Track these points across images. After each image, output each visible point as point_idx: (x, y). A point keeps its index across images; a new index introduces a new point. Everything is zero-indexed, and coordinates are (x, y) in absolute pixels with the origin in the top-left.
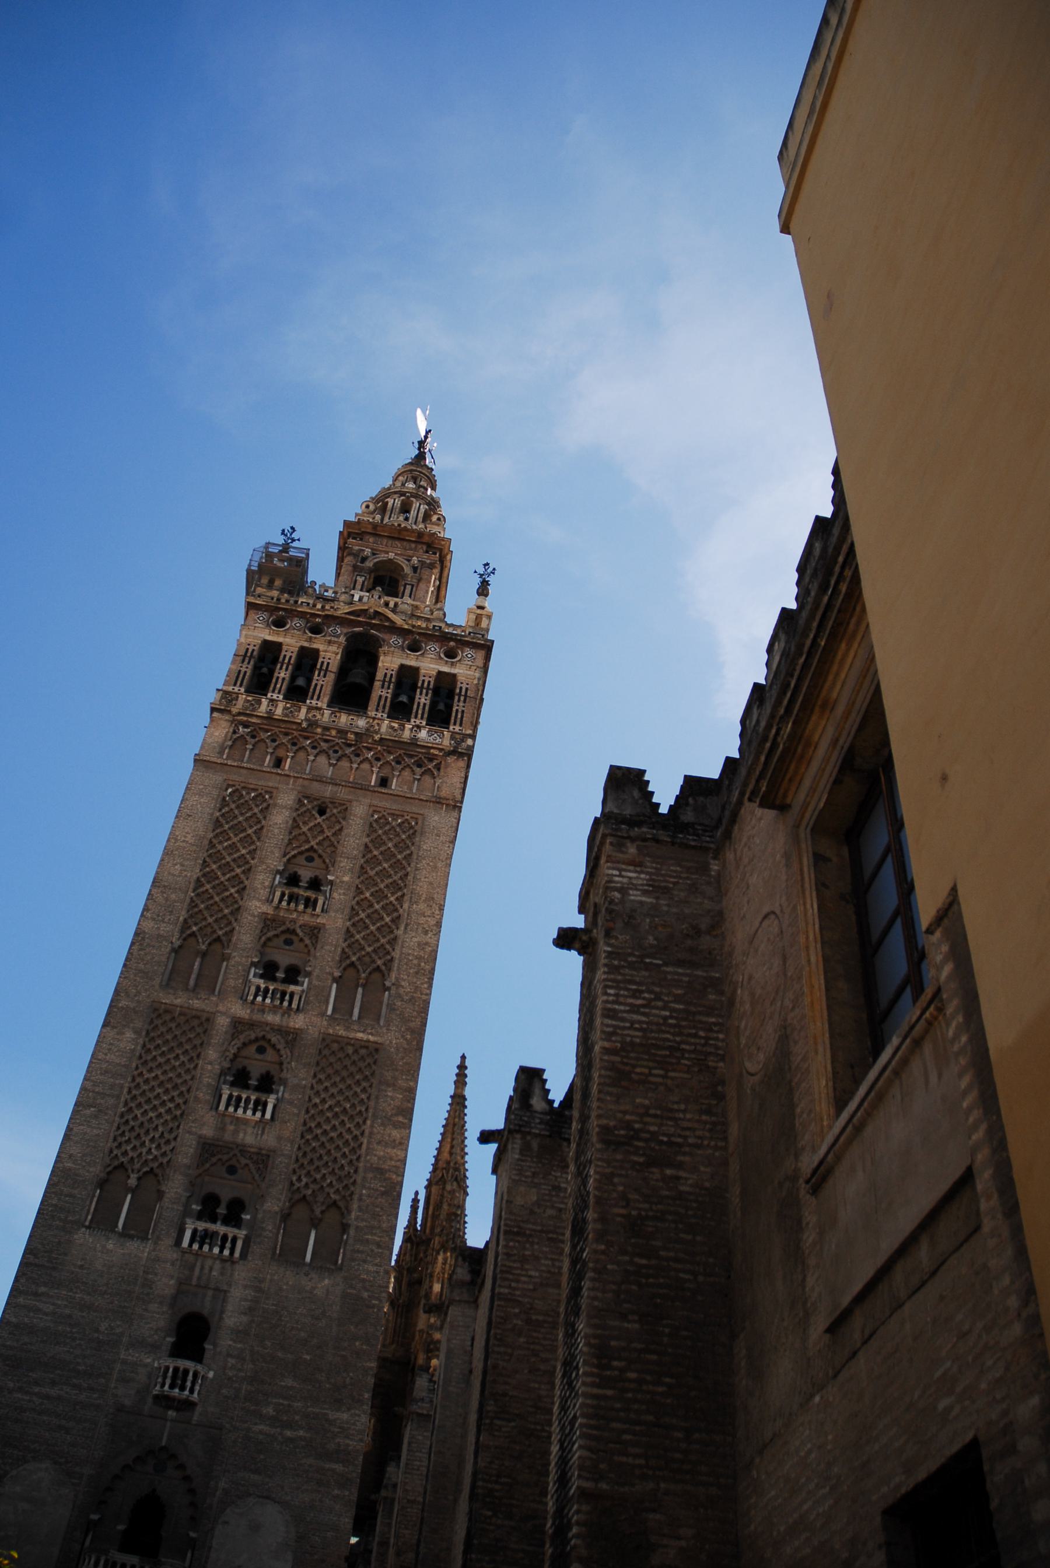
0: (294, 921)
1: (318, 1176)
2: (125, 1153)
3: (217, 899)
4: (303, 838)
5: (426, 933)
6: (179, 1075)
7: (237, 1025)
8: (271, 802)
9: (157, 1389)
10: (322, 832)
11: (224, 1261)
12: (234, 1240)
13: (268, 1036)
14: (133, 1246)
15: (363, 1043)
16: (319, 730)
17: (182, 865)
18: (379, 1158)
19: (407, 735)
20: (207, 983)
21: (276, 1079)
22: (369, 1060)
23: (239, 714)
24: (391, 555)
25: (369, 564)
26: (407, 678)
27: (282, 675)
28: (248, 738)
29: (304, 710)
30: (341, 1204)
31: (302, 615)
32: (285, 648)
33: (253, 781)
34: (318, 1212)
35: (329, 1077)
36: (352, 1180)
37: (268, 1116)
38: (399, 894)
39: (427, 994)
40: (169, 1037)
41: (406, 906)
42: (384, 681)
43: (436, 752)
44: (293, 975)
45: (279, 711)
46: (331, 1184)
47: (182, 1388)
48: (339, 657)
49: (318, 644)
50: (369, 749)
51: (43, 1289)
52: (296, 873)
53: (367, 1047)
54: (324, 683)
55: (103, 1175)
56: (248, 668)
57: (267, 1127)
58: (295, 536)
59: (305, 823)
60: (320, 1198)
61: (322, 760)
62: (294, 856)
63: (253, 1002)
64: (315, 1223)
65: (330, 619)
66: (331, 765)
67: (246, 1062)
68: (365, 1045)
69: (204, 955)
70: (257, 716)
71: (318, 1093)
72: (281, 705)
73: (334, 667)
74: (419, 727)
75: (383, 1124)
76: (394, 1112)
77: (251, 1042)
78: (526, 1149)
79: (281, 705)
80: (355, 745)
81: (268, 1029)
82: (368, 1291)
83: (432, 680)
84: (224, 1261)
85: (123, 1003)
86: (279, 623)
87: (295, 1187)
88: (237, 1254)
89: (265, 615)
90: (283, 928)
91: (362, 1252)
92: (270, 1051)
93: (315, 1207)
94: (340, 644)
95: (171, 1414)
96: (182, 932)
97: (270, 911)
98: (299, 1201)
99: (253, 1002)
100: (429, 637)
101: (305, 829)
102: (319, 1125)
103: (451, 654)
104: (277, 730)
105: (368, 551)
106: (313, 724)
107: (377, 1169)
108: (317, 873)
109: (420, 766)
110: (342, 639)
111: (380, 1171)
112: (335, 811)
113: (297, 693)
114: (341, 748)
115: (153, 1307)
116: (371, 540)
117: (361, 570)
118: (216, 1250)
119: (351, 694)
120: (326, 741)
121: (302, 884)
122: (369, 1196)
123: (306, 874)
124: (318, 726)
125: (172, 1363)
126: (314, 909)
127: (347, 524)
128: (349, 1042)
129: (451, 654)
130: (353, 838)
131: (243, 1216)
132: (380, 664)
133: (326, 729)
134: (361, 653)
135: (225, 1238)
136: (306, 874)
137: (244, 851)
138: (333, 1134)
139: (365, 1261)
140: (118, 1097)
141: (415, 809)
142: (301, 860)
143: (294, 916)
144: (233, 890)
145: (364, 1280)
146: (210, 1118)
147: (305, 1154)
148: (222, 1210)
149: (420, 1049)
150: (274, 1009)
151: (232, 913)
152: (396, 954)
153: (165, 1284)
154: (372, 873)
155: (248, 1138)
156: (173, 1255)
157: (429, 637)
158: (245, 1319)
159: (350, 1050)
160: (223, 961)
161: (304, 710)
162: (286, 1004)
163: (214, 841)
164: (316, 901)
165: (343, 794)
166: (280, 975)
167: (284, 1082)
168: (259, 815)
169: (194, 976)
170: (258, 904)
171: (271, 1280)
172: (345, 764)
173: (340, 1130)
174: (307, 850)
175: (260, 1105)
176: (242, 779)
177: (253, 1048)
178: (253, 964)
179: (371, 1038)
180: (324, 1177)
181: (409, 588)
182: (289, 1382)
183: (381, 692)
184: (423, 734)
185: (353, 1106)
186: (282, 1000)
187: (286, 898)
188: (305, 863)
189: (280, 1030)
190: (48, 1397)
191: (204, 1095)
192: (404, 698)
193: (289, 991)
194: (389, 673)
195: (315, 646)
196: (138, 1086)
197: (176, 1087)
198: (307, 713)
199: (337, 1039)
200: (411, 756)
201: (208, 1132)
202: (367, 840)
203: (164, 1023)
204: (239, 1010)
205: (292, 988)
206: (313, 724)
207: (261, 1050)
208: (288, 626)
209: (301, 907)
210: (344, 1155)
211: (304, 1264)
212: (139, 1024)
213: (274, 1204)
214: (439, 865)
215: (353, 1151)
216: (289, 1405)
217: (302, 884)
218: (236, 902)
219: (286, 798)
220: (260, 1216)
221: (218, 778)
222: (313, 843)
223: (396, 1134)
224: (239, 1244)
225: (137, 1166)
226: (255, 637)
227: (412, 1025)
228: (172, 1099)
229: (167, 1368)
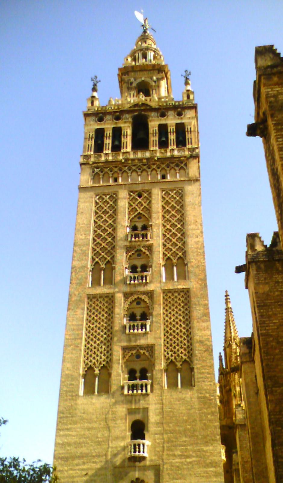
0: (139, 246)
1: (176, 350)
4: (134, 210)
8: (116, 198)
10: (142, 205)
12: (146, 385)
13: (140, 297)
15: (181, 290)
16: (130, 162)
17: (85, 234)
18: (200, 336)
19: (169, 154)
21: (148, 314)
23: (93, 163)
24: (143, 79)
25: (134, 85)
26: (163, 130)
28: (100, 173)
29: (121, 155)
31: (110, 113)
35: (170, 308)
36: (190, 348)
37: (148, 329)
38: (182, 223)
39: (204, 263)
42: (153, 134)
43: (183, 159)
44: (145, 268)
46: (182, 353)
47: (139, 452)
48: (131, 127)
49: (121, 124)
50: (154, 164)
52: (135, 225)
53: (183, 291)
54: (127, 141)
58: (98, 80)
60: (178, 359)
61: (134, 174)
62: (133, 218)
64: (178, 371)
65: (123, 112)
66: (139, 175)
68: (182, 290)
70: (101, 163)
71: (167, 316)
74: (173, 150)
75: (198, 322)
76: (201, 315)
77: (133, 301)
78: (258, 269)
80: (147, 164)
81: (139, 293)
82: (208, 393)
83: (174, 128)
86: (101, 120)
87: (167, 357)
89: (94, 118)
90: (135, 250)
91: (202, 378)
93: (177, 363)
96: (92, 262)
97: (128, 244)
98: (170, 363)
103: (180, 114)
104: (111, 166)
105: (132, 80)
106: (127, 160)
107: (200, 341)
108: (144, 223)
110: (130, 120)
111: (201, 342)
112: (145, 195)
114: (141, 167)
119: (140, 142)
120: (134, 165)
122: (199, 353)
123: (139, 225)
126: (147, 238)
127: (120, 69)
129: (180, 114)
131: (148, 375)
136: (139, 225)
139: (204, 381)
141: (180, 186)
142: (136, 219)
143: (139, 243)
145: (205, 390)
146: (123, 337)
147: (168, 343)
148: (138, 375)
150: (140, 284)
151: (112, 249)
155: (142, 342)
160: (113, 270)
164: (147, 235)
165: (146, 188)
166: (139, 270)
170: (122, 242)
171: (166, 399)
174: (137, 214)
175: (144, 326)
177: (135, 303)
179: (184, 287)
180: (178, 350)
183: (154, 139)
186: (142, 280)
187: (133, 236)
188: (138, 220)
189: (144, 293)
192: (164, 139)
193: (144, 275)
195: (119, 125)
198: (123, 155)
199: (170, 291)
200: (173, 163)
205: (145, 273)
206: (127, 160)
207: (138, 303)
208: (105, 120)
209: (141, 239)
214: (196, 207)
216: (186, 449)
218: (112, 244)
220: (154, 373)
223: (205, 324)
224: (149, 387)
226: (91, 129)
227: (200, 277)
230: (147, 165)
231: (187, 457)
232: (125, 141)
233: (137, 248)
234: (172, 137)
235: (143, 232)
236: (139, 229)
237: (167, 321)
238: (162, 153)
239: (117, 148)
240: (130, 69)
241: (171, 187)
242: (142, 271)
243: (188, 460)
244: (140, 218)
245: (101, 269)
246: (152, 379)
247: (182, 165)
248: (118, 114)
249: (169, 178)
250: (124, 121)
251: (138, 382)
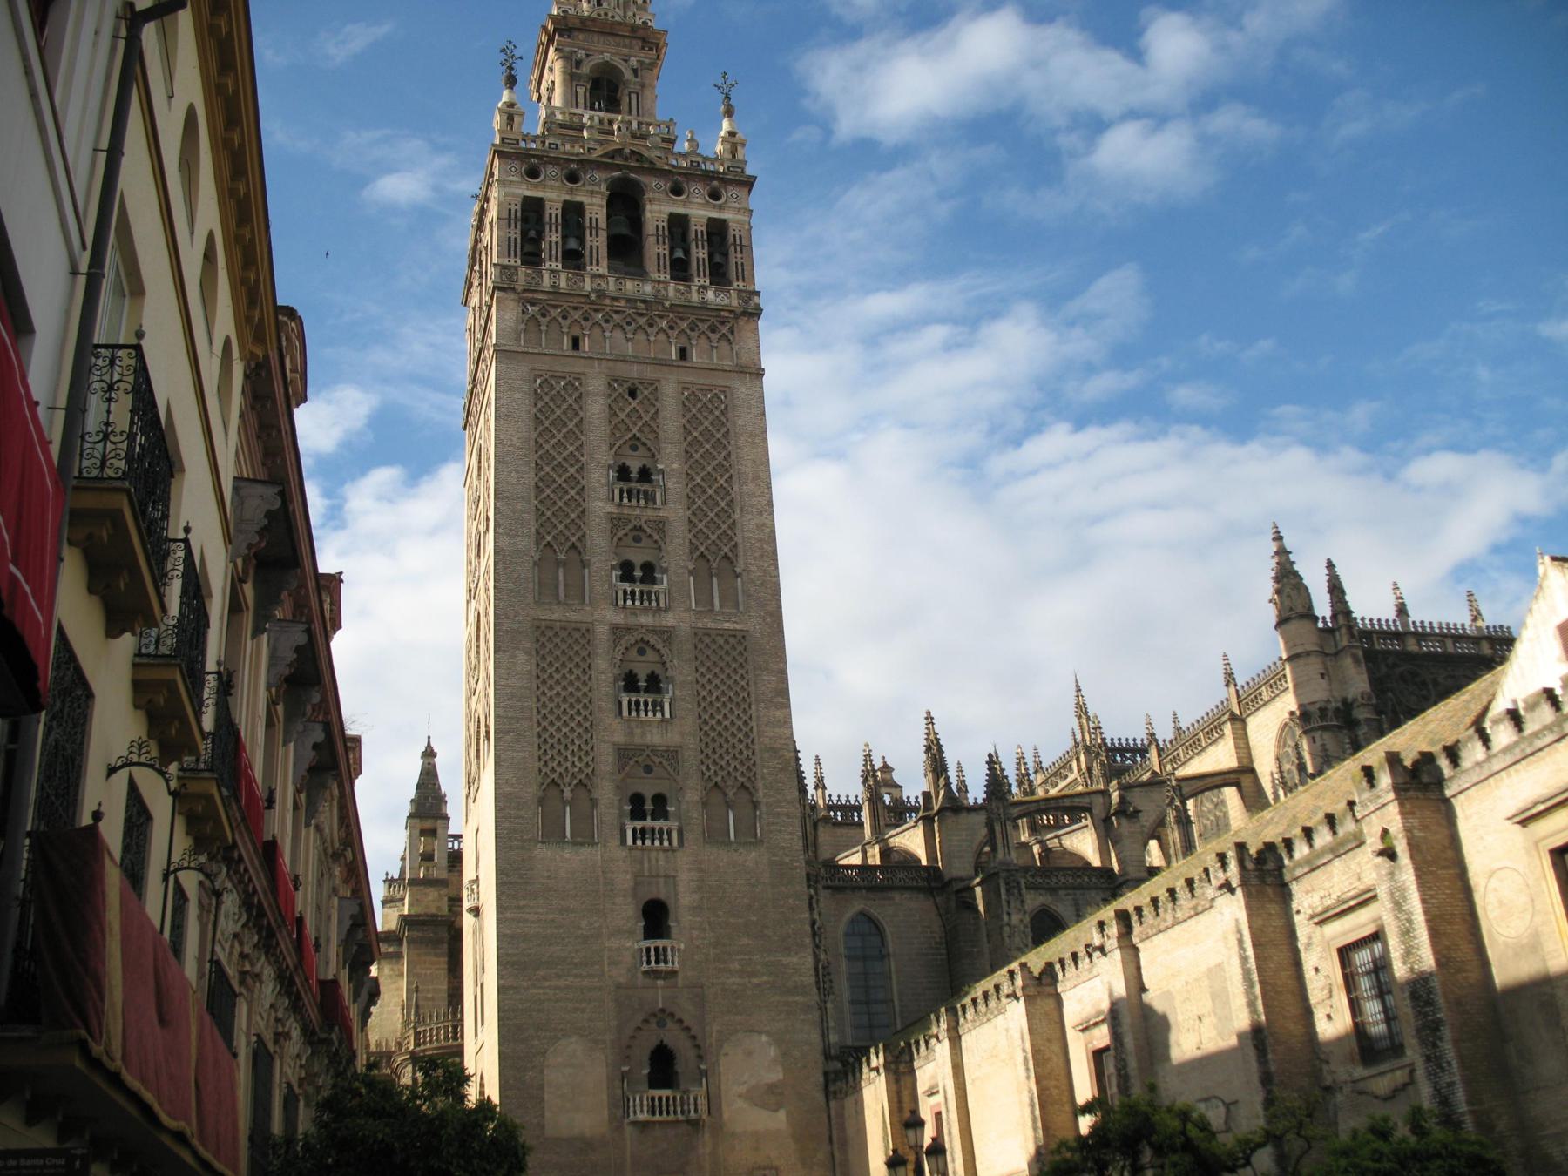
0: (638, 517)
2: (553, 770)
3: (560, 504)
5: (761, 513)
6: (578, 689)
7: (617, 631)
9: (645, 967)
10: (640, 417)
11: (665, 851)
12: (669, 833)
14: (585, 851)
16: (607, 301)
19: (695, 298)
20: (578, 593)
22: (740, 648)
23: (525, 291)
24: (607, 56)
25: (585, 70)
26: (678, 225)
27: (554, 239)
29: (587, 280)
30: (748, 785)
31: (555, 161)
32: (548, 205)
33: (560, 367)
34: (730, 793)
37: (667, 715)
40: (558, 653)
41: (736, 488)
45: (563, 284)
47: (666, 962)
50: (661, 317)
51: (522, 903)
54: (598, 242)
55: (540, 793)
56: (516, 234)
57: (672, 725)
59: (622, 410)
60: (730, 783)
61: (618, 334)
63: (624, 607)
64: (729, 805)
66: (628, 340)
67: (632, 666)
69: (564, 564)
72: (563, 276)
73: (603, 224)
74: (704, 287)
79: (563, 276)
84: (665, 851)
85: (506, 626)
88: (675, 843)
89: (517, 164)
92: (649, 651)
94: (602, 194)
95: (660, 982)
96: (537, 544)
99: (624, 607)
100: (689, 176)
101: (622, 416)
102: (712, 716)
105: (581, 54)
106: (601, 294)
108: (645, 462)
109: (713, 331)
110: (603, 188)
111: (773, 750)
113: (573, 259)
115: (619, 900)
116: (581, 36)
117: (579, 77)
118: (657, 843)
119: (626, 249)
120: (617, 312)
121: (635, 479)
123: (634, 466)
124: (605, 296)
125: (652, 944)
128: (721, 633)
130: (671, 423)
132: (648, 215)
133: (613, 299)
134: (626, 201)
135: (661, 831)
136: (634, 466)
137: (571, 449)
138: (727, 723)
140: (531, 719)
143: (638, 512)
144: (573, 493)
146: (616, 724)
148: (649, 806)
149: (782, 631)
150: (645, 610)
152: (739, 539)
153: (624, 880)
154: (697, 456)
155: (655, 738)
156: (621, 853)
157: (689, 176)
158: (696, 896)
159: (721, 641)
161: (587, 280)
162: (654, 604)
163: (540, 441)
165: (649, 373)
167: (670, 680)
168: (576, 406)
169: (561, 588)
170: (600, 504)
172: (641, 336)
173: (732, 717)
175: (658, 705)
176: (546, 367)
177: (634, 651)
178: (613, 567)
179: (738, 627)
181: (634, 96)
182: (745, 941)
183: (655, 250)
184: (710, 295)
185: (737, 694)
186: (650, 601)
190: (557, 988)
191: (606, 704)
194: (660, 225)
195: (578, 199)
196: (544, 705)
197: (578, 700)
199: (707, 632)
200: (703, 321)
201: (620, 738)
202: (684, 421)
203: (550, 639)
204: (614, 617)
205: (656, 587)
207: (641, 652)
209: (642, 502)
210: (740, 741)
211: (729, 843)
212: (527, 644)
213: (691, 795)
215: (746, 735)
217: (635, 479)
219: (596, 384)
220: (684, 806)
221: (521, 370)
222: (635, 431)
223: (779, 714)
224: (675, 835)
225: (567, 780)
226: (514, 195)
227: (769, 608)
228: (578, 712)
229: (648, 950)
230: (646, 313)
231: (753, 974)
232: (595, 244)
233: (634, 522)
234: (700, 253)
235: (646, 486)
236: (634, 475)
237: (704, 698)
238: (678, 291)
239: (573, 259)
240: (578, 25)
241: (702, 380)
242: (642, 581)
243: (755, 981)
244: (634, 448)
245: (558, 563)
246: (679, 818)
247: (725, 330)
248: (574, 166)
249: (694, 355)
250: (590, 188)
251: (649, 823)
